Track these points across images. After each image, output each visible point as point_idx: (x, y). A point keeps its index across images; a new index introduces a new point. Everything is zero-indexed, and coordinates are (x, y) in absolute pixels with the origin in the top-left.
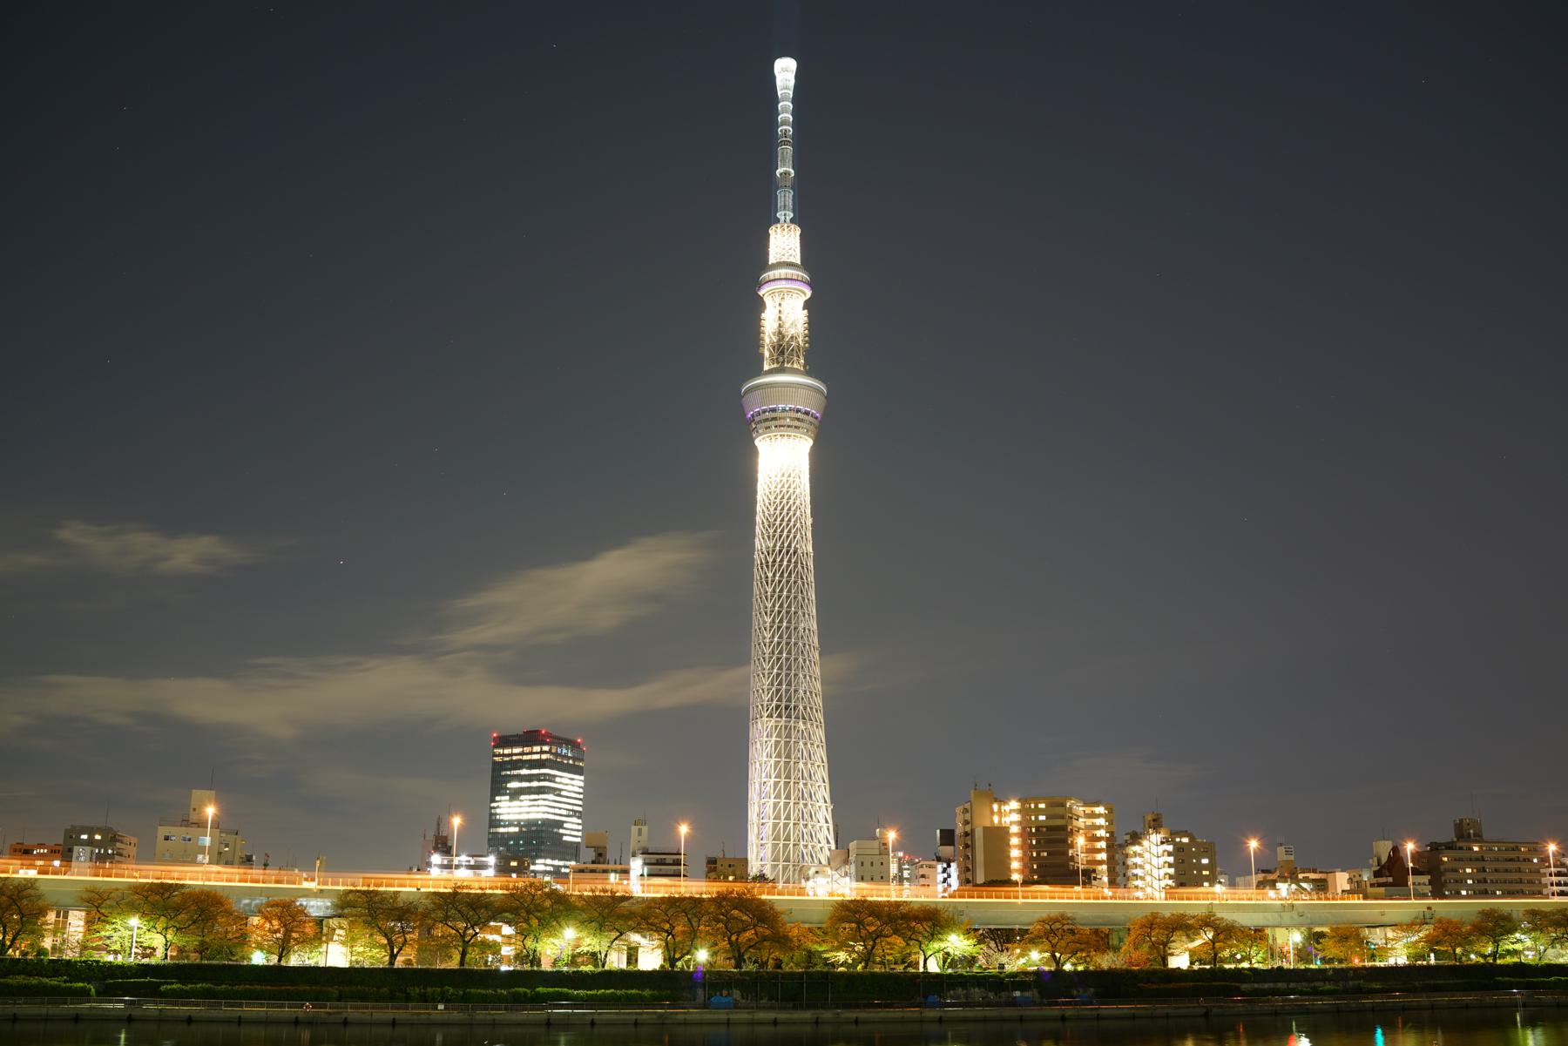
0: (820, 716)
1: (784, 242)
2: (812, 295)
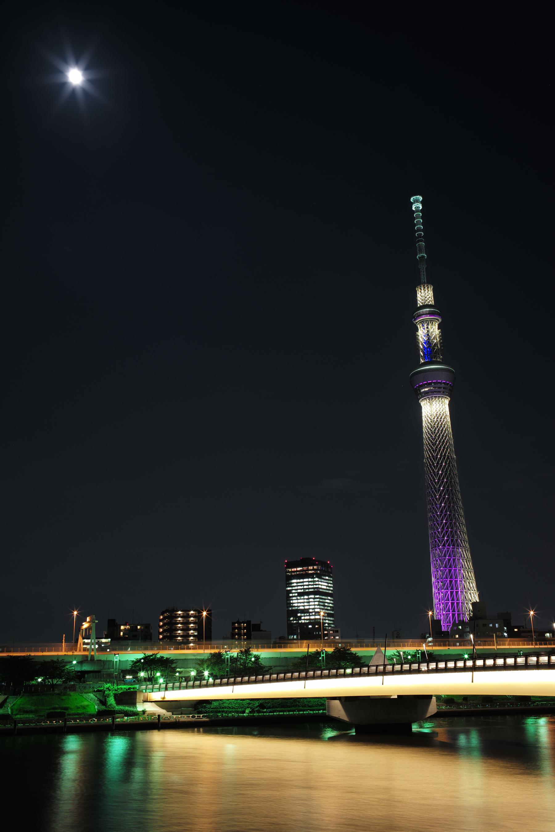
0: (468, 546)
2: (442, 320)
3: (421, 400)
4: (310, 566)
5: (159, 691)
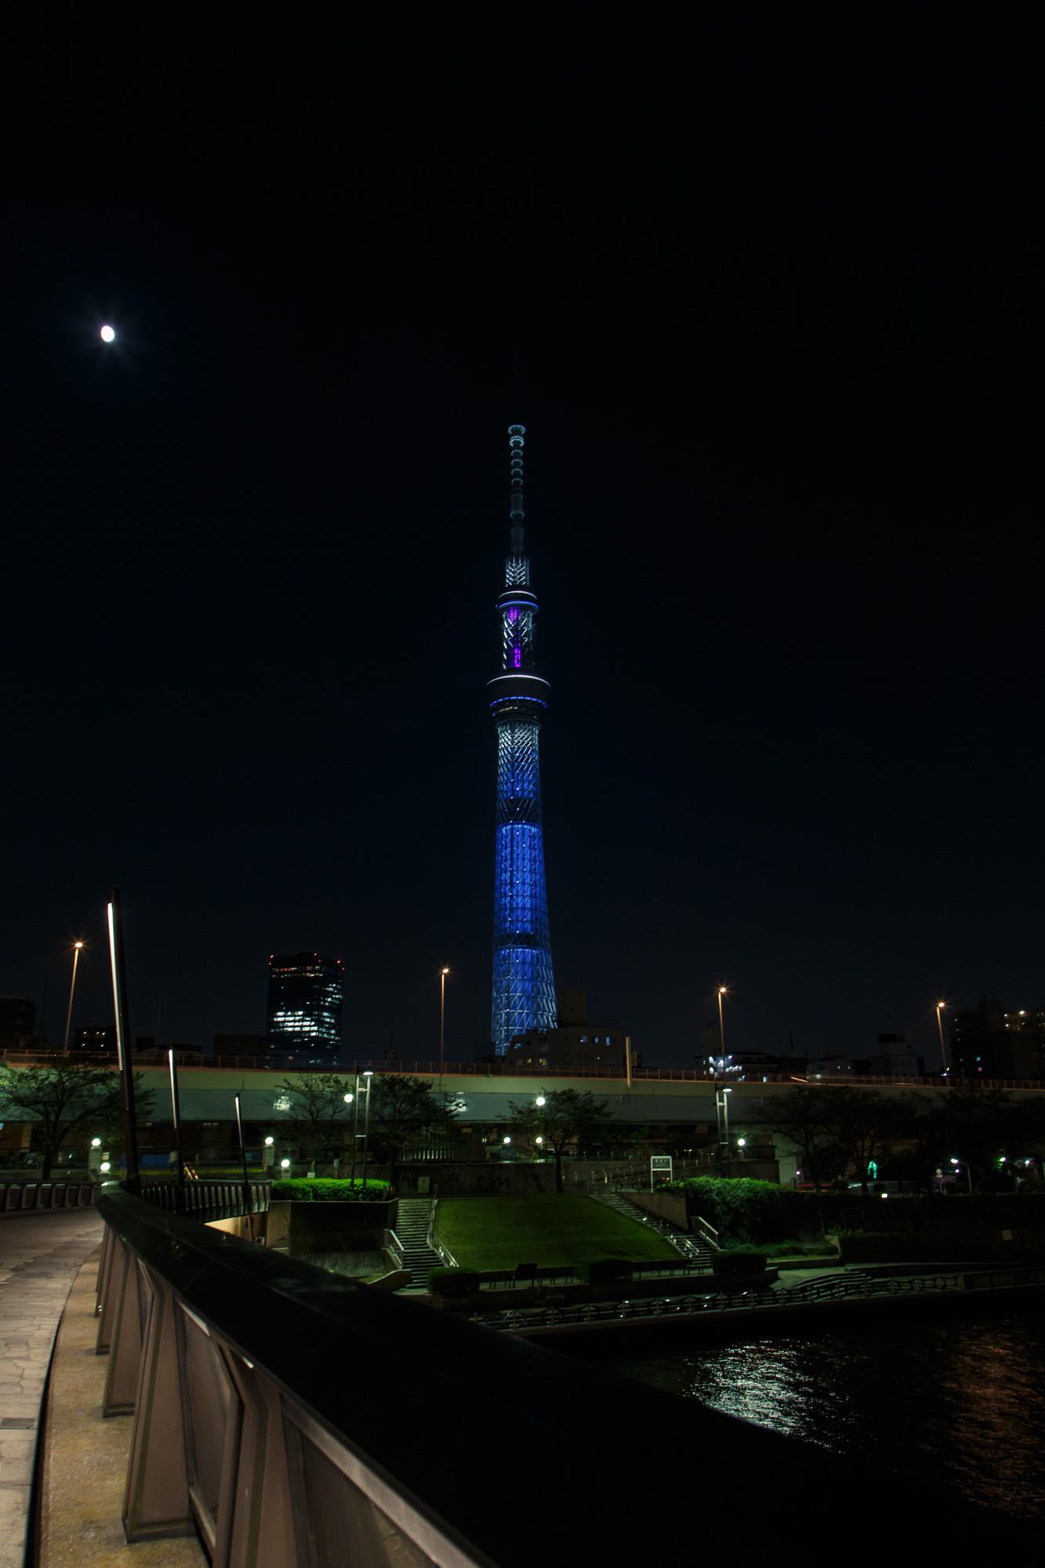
0: (548, 944)
1: (516, 572)
3: (498, 724)
4: (310, 965)
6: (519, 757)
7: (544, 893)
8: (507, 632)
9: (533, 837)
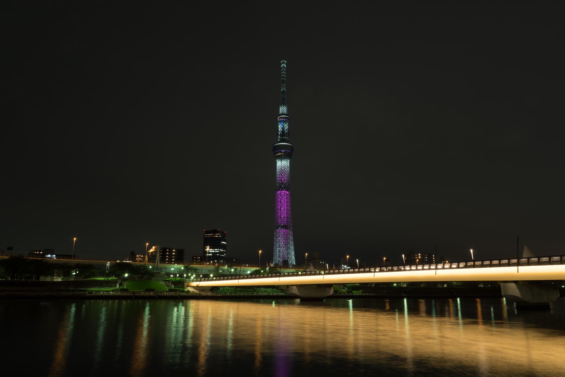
0: (292, 229)
4: (216, 233)
5: (193, 282)
6: (283, 169)
7: (290, 212)
8: (280, 129)
9: (287, 195)
